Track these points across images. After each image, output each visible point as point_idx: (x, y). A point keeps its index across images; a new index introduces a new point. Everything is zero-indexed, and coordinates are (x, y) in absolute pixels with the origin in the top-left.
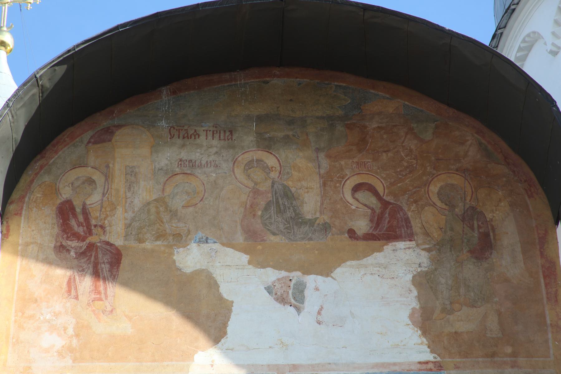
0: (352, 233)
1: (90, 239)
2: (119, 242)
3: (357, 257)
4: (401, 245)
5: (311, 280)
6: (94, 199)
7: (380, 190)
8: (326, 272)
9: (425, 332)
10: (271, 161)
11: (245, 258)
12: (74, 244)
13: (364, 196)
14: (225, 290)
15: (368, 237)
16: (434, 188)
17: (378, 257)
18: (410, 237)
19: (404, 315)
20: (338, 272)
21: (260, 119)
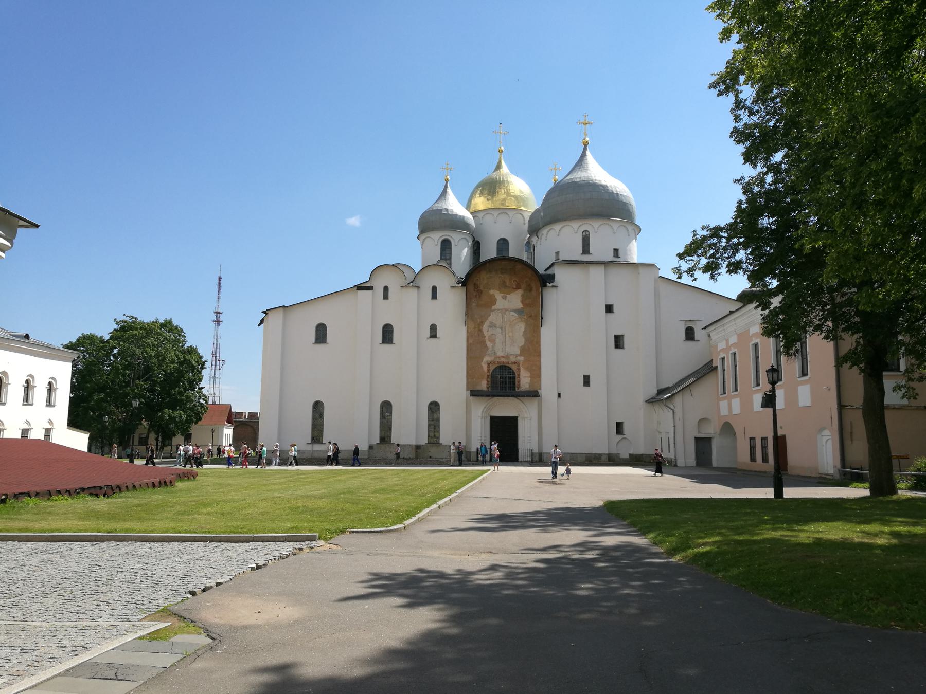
0: (513, 288)
1: (479, 289)
2: (482, 289)
3: (514, 291)
4: (520, 290)
5: (507, 295)
6: (479, 283)
7: (517, 280)
8: (509, 294)
9: (522, 303)
10: (502, 276)
11: (498, 292)
12: (476, 290)
13: (515, 282)
14: (496, 297)
15: (515, 289)
16: (525, 280)
17: (517, 292)
18: (520, 288)
19: (519, 301)
20: (512, 294)
21: (501, 269)
